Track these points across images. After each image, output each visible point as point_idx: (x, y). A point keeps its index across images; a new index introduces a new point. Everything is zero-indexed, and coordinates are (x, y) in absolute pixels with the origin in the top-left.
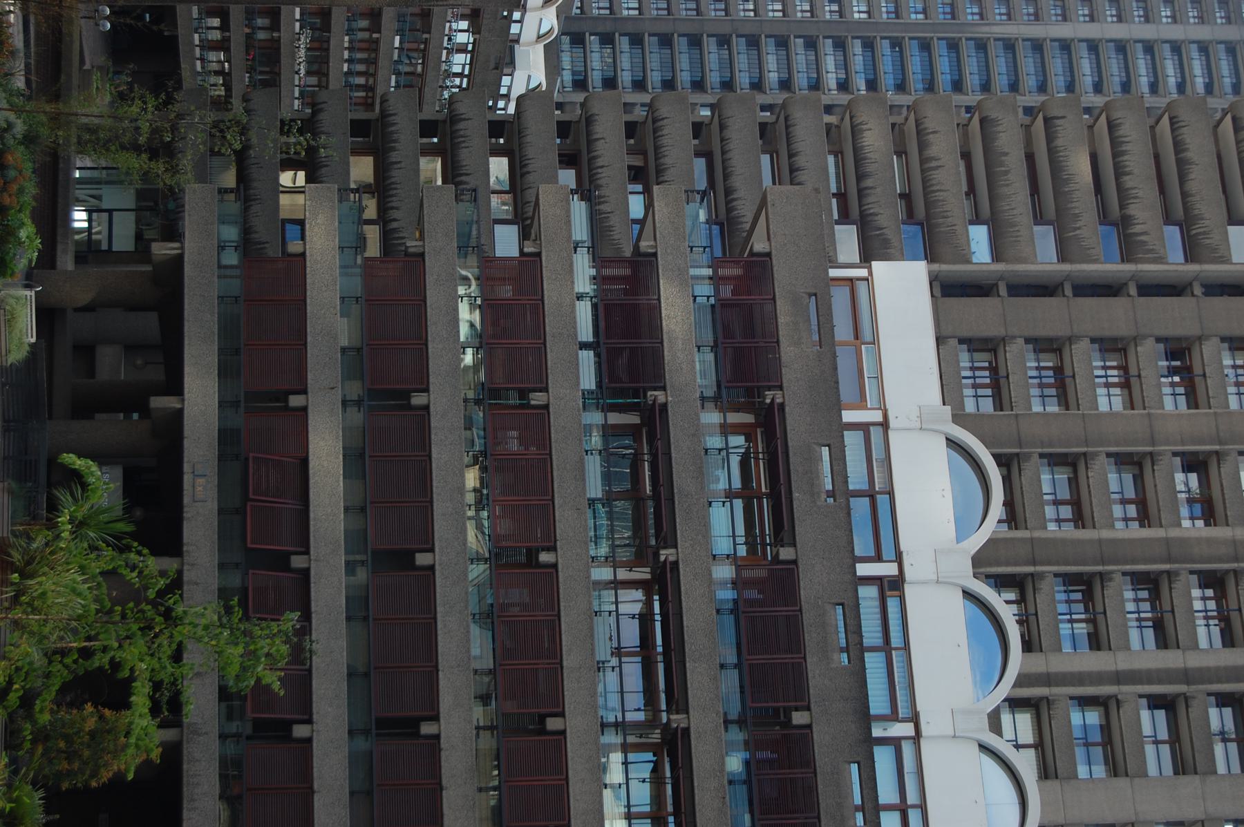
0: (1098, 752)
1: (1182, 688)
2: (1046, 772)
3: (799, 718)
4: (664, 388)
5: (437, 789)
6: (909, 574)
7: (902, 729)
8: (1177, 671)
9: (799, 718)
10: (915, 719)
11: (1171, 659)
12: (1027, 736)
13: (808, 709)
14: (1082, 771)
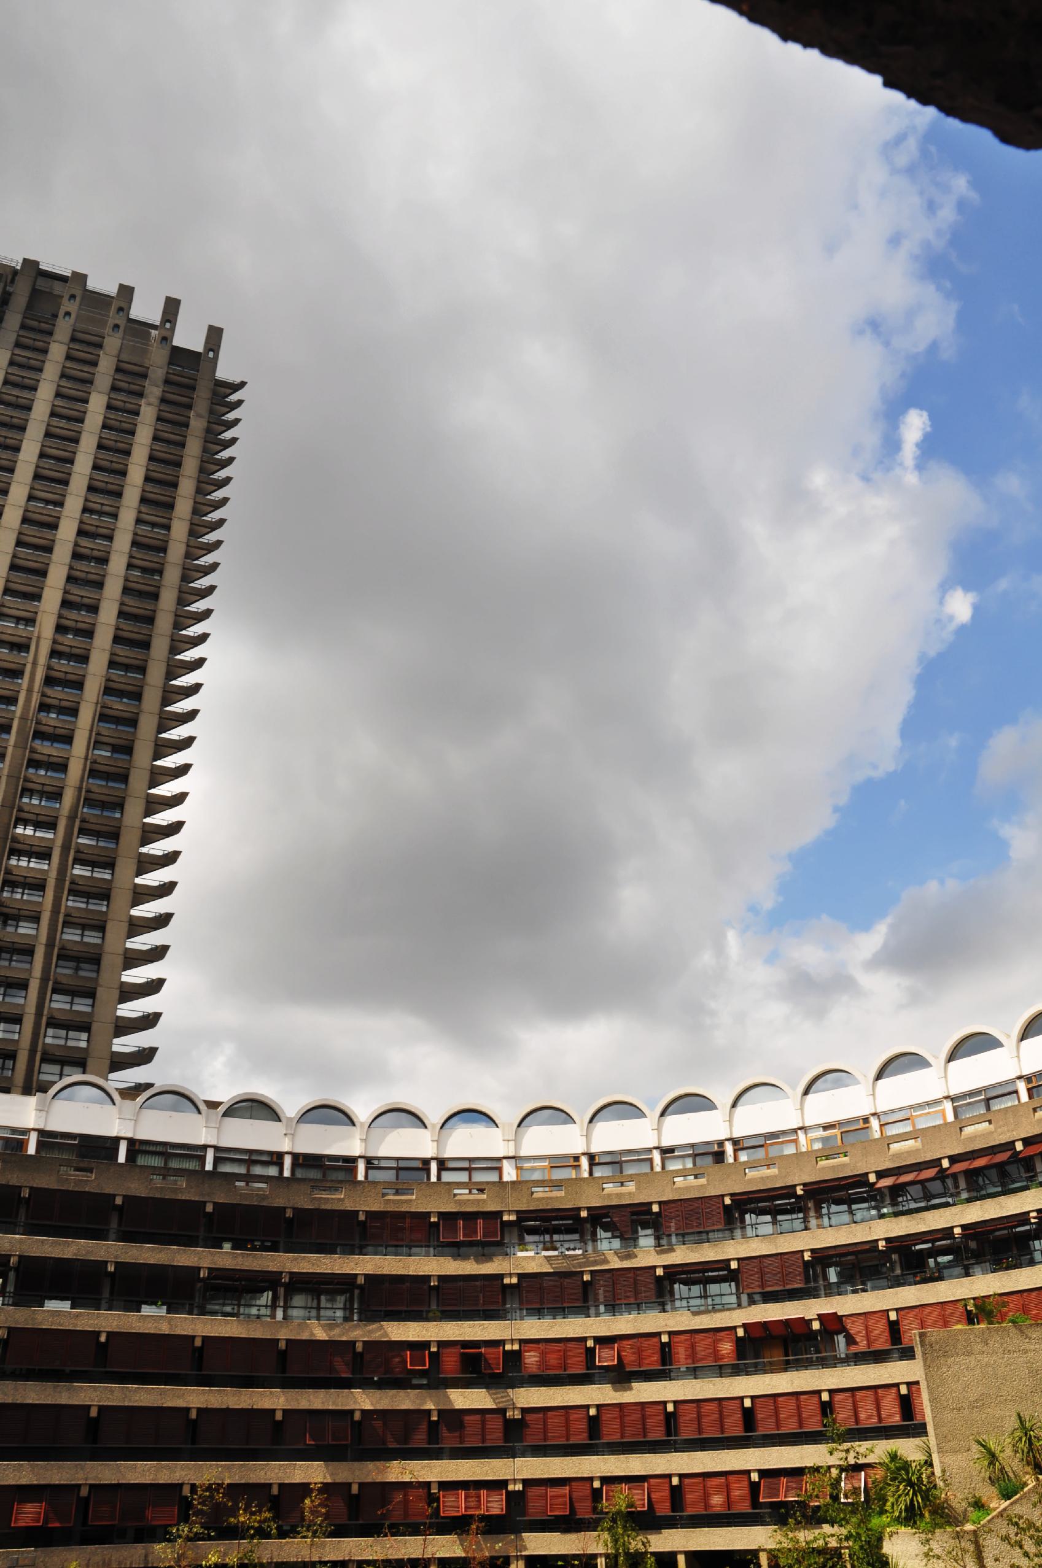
0: (72, 1034)
1: (51, 983)
2: (80, 1062)
3: (209, 1208)
4: (10, 1256)
5: (228, 1411)
6: (130, 1135)
7: (210, 1156)
8: (41, 983)
9: (209, 1208)
10: (205, 1147)
11: (34, 985)
12: (56, 1069)
13: (205, 1203)
14: (83, 1044)
